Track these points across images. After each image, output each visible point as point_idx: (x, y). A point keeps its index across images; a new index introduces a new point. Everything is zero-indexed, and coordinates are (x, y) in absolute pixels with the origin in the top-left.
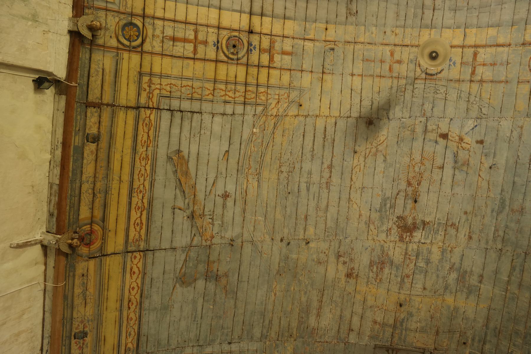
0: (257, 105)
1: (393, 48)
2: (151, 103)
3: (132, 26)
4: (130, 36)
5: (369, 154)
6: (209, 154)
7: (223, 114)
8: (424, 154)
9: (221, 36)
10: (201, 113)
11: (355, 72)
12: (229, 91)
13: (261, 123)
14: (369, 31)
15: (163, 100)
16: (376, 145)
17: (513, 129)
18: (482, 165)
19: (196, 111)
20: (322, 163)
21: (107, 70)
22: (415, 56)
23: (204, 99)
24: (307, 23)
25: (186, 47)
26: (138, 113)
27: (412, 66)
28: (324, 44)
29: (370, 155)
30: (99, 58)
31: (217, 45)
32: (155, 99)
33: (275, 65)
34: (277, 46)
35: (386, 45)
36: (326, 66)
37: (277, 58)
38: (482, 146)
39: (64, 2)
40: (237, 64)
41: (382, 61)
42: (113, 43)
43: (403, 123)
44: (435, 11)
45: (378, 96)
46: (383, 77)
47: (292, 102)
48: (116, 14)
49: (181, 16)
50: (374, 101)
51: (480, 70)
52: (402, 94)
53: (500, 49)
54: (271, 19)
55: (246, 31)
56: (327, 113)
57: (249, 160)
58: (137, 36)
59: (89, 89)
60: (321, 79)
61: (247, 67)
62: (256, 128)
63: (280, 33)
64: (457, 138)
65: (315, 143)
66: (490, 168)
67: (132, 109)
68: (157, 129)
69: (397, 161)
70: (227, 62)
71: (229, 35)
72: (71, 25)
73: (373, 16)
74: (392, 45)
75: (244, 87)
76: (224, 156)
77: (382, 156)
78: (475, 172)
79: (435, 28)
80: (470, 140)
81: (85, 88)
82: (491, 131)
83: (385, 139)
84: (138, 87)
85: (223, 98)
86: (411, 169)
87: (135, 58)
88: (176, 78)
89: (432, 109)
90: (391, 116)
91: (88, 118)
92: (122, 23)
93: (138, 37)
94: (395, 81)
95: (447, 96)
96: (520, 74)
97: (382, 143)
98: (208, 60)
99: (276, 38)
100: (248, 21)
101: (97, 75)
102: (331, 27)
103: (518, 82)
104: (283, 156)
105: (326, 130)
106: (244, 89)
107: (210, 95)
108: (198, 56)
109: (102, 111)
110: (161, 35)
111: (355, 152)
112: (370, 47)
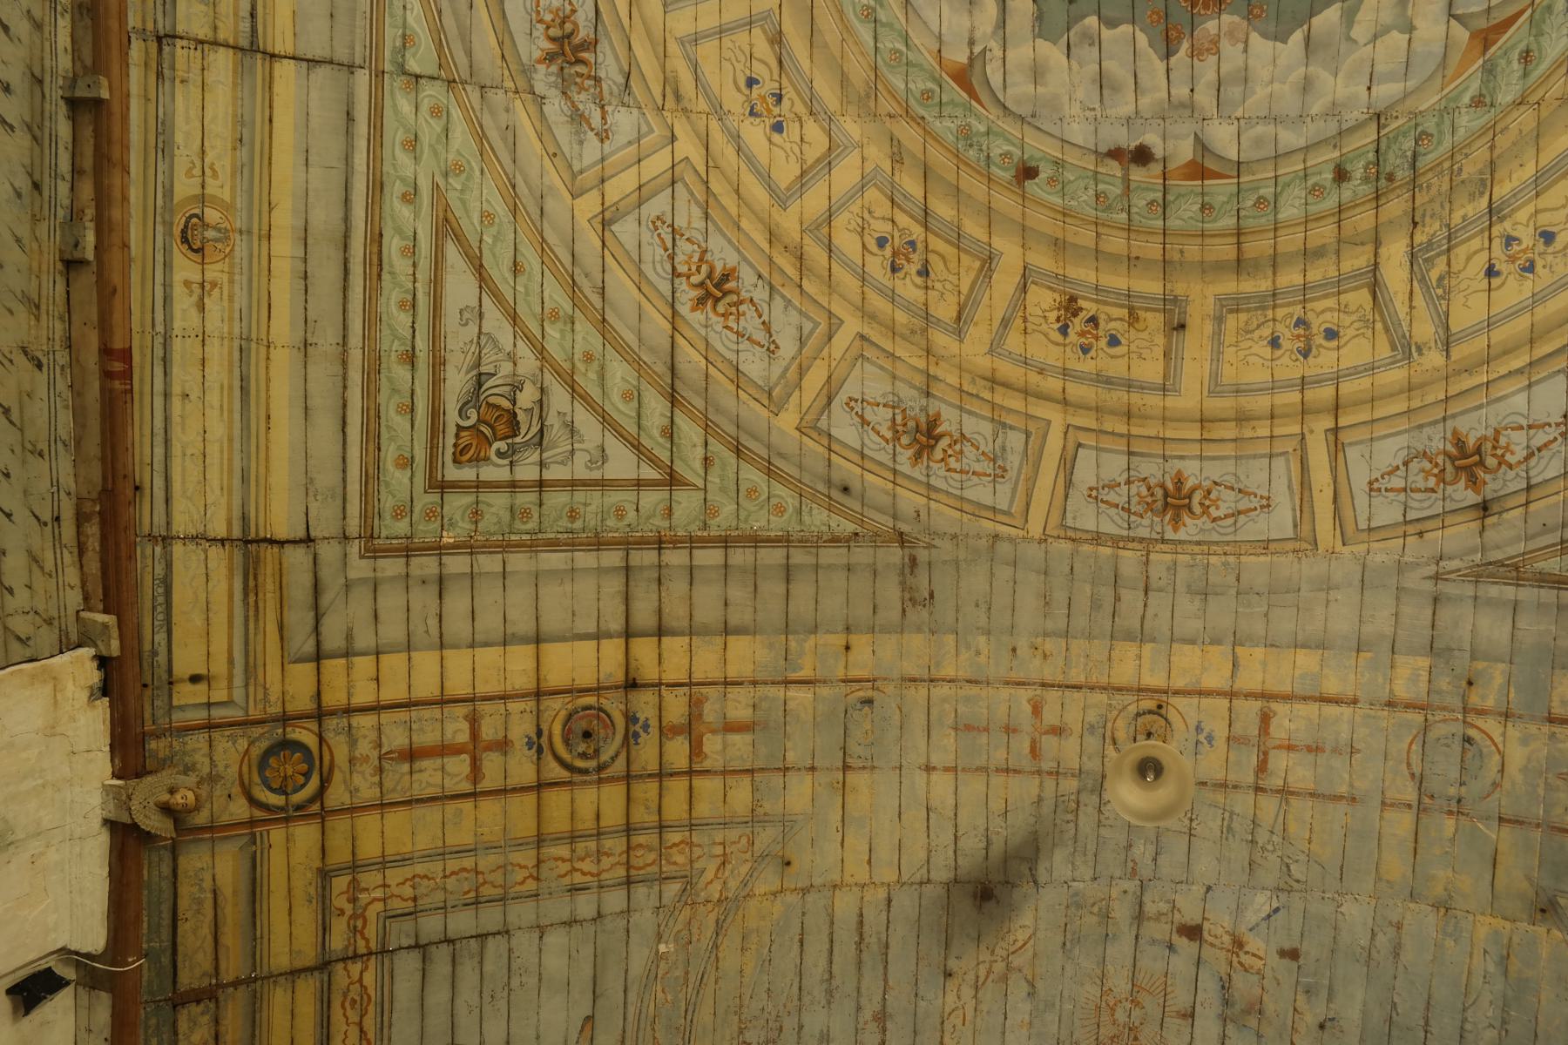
0: (664, 879)
1: (1038, 692)
2: (361, 943)
3: (287, 752)
4: (285, 777)
5: (987, 977)
6: (538, 1037)
7: (570, 923)
8: (1140, 976)
9: (547, 716)
10: (507, 932)
11: (936, 760)
12: (583, 860)
13: (679, 926)
14: (968, 647)
15: (394, 926)
16: (1004, 954)
17: (1376, 929)
18: (1297, 1016)
19: (495, 929)
20: (859, 1008)
21: (227, 891)
22: (1101, 716)
23: (512, 895)
24: (790, 637)
25: (449, 768)
26: (326, 978)
27: (1092, 742)
28: (843, 689)
29: (990, 979)
30: (199, 865)
31: (538, 743)
32: (371, 931)
33: (707, 764)
34: (710, 712)
35: (1018, 684)
36: (854, 749)
37: (712, 744)
38: (1294, 965)
39: (85, 748)
40: (600, 781)
41: (1009, 730)
42: (240, 809)
43: (1076, 894)
44: (1150, 593)
45: (1003, 824)
46: (1015, 771)
47: (763, 857)
48: (238, 731)
49: (426, 686)
50: (994, 838)
51: (1279, 761)
52: (1070, 817)
53: (1331, 710)
54: (687, 639)
55: (617, 687)
56: (862, 875)
57: (653, 1029)
58: (303, 775)
59: (180, 958)
60: (840, 785)
61: (628, 784)
62: (667, 943)
63: (716, 675)
64: (1227, 939)
65: (836, 958)
66: (1322, 1027)
67: (308, 974)
68: (385, 1008)
69: (1066, 994)
70: (570, 783)
71: (569, 706)
72: (111, 806)
73: (977, 605)
74: (1034, 684)
75: (625, 839)
76: (581, 1031)
77: (1025, 984)
78: (1281, 1036)
79: (1153, 640)
80: (1262, 945)
81: (166, 960)
82: (1319, 927)
83: (1030, 938)
84: (320, 911)
85: (567, 880)
86: (1105, 1017)
87: (305, 834)
88: (428, 857)
89: (1155, 860)
90: (1042, 876)
91: (180, 1037)
92: (256, 751)
93: (307, 775)
94: (1050, 783)
95: (1194, 825)
96: (1387, 784)
97: (1021, 948)
98: (514, 790)
99: (704, 690)
100: (621, 657)
101: (198, 912)
102: (860, 642)
103: (1383, 803)
104: (746, 1002)
105: (861, 922)
106: (625, 843)
107: (530, 881)
108: (486, 784)
109: (222, 1004)
110: (375, 754)
111: (948, 975)
112: (974, 690)
